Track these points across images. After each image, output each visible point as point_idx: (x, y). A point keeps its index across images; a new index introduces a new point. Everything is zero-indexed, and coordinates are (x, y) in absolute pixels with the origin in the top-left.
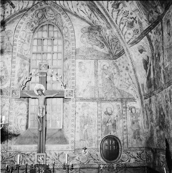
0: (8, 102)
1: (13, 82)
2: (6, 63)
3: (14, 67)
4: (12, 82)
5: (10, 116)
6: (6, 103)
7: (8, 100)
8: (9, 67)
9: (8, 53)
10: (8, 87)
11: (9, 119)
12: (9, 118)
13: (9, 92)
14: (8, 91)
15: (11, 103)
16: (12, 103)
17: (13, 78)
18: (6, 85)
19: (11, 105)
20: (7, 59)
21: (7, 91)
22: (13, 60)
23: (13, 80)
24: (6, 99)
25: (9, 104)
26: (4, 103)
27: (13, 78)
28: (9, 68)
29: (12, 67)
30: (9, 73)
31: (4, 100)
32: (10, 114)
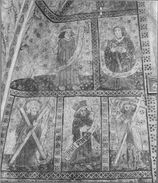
0: (143, 103)
1: (148, 63)
2: (127, 30)
3: (145, 35)
4: (146, 63)
5: (150, 133)
6: (138, 105)
7: (141, 98)
8: (134, 36)
9: (129, 12)
10: (137, 72)
11: (151, 139)
12: (150, 137)
13: (141, 83)
14: (139, 82)
15: (151, 105)
16: (152, 105)
17: (145, 55)
18: (133, 69)
19: (149, 109)
20: (129, 21)
21: (137, 82)
22: (142, 23)
23: (147, 59)
24: (138, 98)
25: (146, 107)
26: (134, 107)
27: (147, 55)
28: (136, 37)
29: (141, 35)
30: (137, 47)
31: (132, 100)
32: (151, 128)
